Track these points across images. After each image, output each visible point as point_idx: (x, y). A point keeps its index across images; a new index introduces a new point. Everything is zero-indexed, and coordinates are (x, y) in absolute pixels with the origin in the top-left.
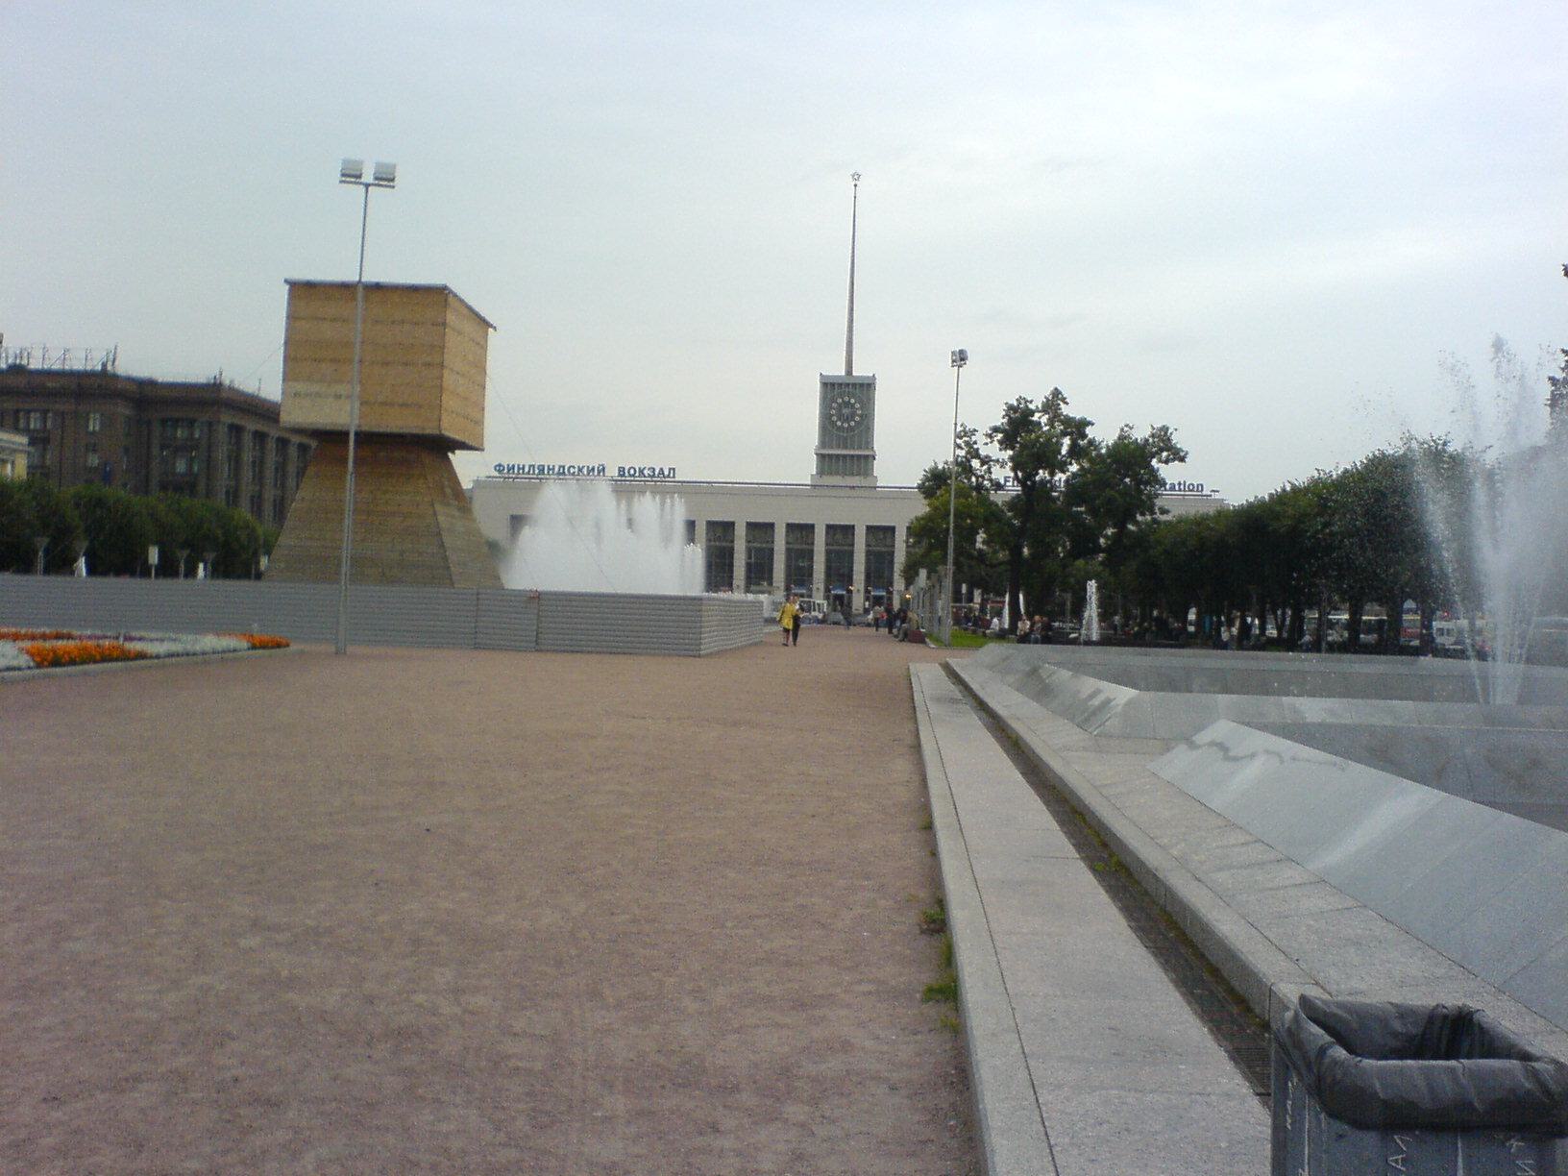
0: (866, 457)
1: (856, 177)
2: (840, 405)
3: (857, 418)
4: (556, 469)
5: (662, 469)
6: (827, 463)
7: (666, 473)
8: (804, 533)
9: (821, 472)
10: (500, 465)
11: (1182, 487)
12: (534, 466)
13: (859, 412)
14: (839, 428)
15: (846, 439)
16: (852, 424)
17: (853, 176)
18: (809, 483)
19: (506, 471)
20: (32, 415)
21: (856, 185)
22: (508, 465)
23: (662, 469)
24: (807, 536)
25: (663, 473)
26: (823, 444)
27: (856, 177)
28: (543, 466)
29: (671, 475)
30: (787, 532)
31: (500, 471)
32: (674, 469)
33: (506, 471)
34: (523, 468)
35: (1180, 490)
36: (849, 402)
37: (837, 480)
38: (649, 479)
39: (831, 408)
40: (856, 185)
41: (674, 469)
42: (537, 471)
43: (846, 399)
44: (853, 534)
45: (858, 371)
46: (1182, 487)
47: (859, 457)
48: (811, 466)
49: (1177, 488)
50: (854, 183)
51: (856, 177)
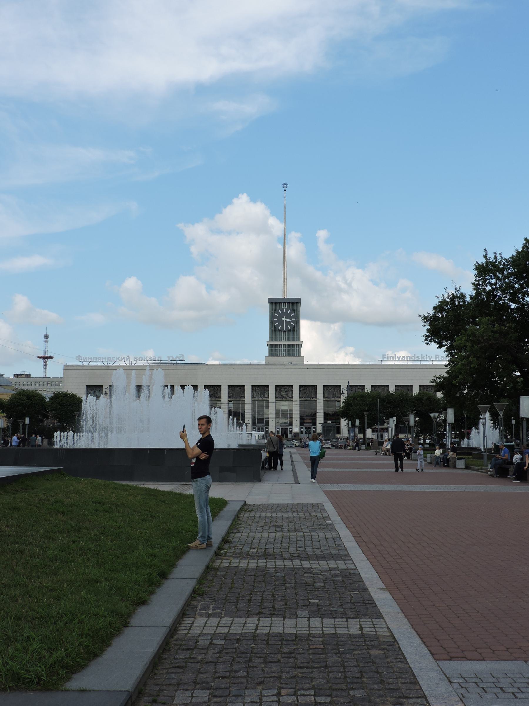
0: (297, 345)
9: (271, 354)
21: (285, 190)
24: (265, 393)
26: (271, 339)
40: (285, 190)
44: (292, 391)
45: (290, 295)
48: (266, 350)
50: (284, 189)
51: (285, 185)
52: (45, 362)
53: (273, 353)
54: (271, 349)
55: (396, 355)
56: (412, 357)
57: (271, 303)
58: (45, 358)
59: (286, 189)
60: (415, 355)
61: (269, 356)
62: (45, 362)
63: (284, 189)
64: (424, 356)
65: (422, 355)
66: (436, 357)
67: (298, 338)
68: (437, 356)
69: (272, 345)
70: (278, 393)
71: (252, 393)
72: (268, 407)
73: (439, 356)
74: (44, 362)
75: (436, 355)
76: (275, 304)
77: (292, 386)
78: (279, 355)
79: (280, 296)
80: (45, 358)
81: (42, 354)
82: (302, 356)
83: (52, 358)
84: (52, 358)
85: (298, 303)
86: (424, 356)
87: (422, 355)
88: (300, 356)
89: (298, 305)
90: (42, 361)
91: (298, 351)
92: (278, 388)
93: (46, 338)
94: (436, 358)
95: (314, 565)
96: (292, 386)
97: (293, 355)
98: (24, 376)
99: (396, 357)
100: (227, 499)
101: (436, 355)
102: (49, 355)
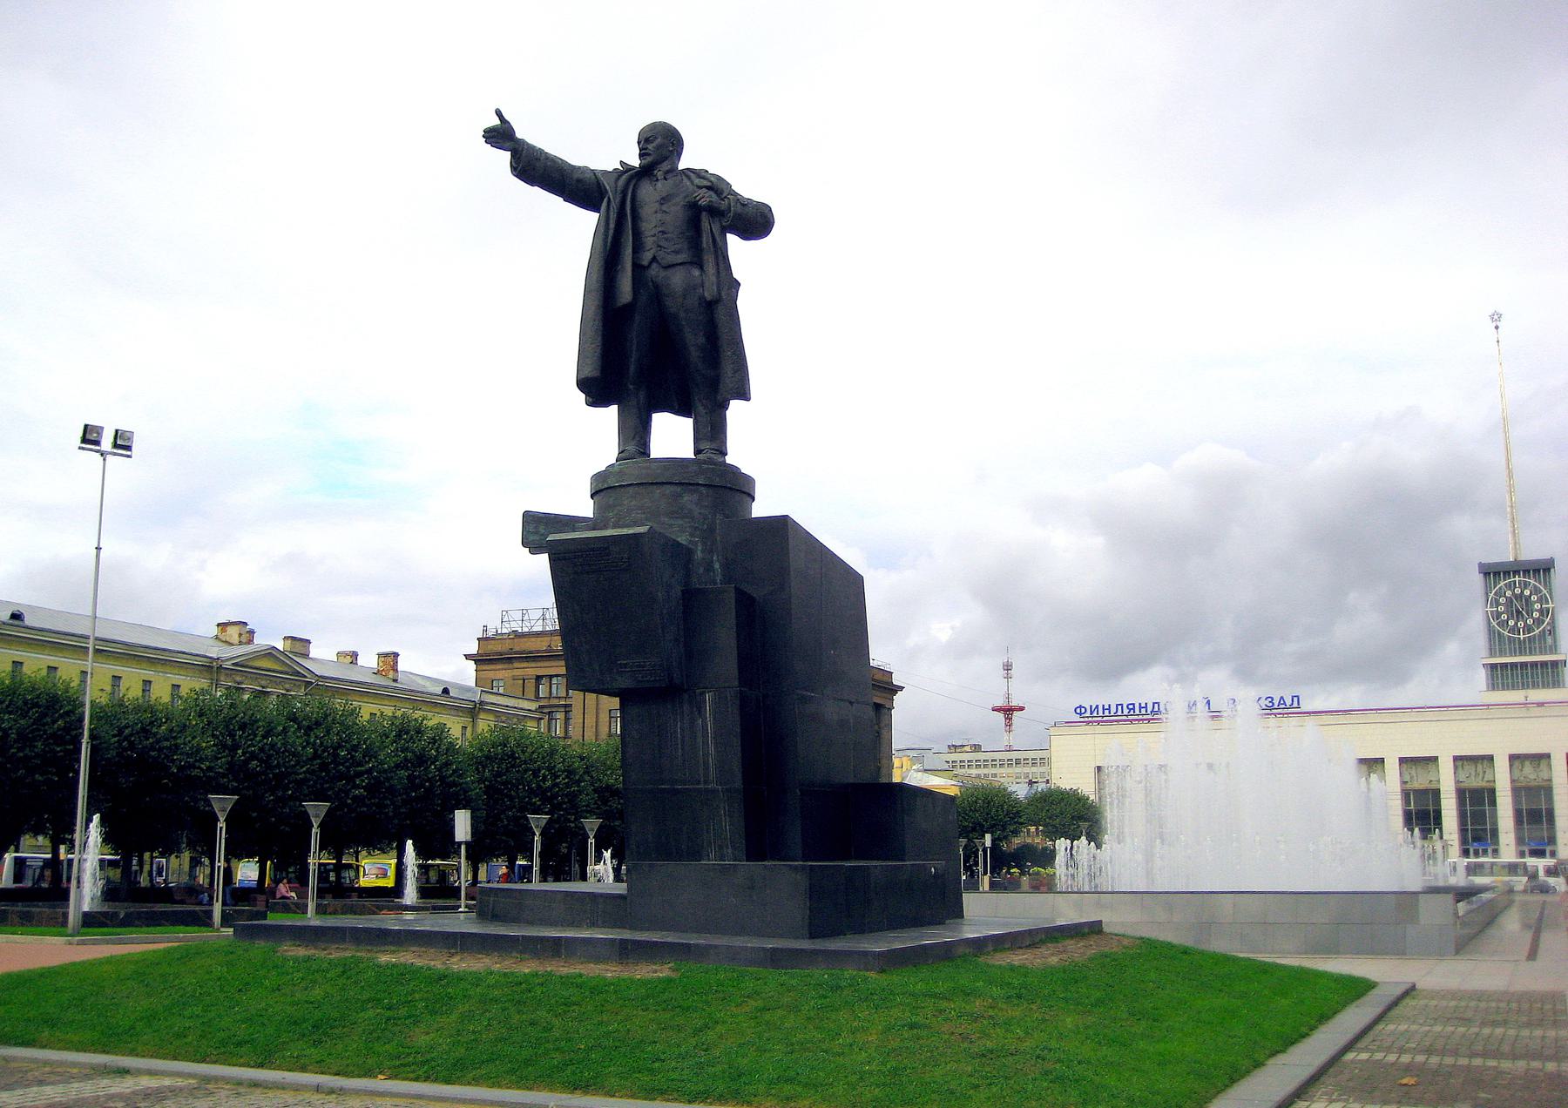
0: (1555, 664)
2: (1510, 601)
3: (1536, 615)
4: (1150, 709)
5: (1282, 698)
6: (1500, 676)
7: (1288, 702)
8: (1479, 766)
9: (1493, 686)
10: (1080, 707)
12: (1121, 705)
14: (1516, 629)
19: (1088, 714)
20: (554, 680)
22: (1091, 706)
23: (1282, 698)
25: (1285, 704)
27: (1496, 317)
28: (1133, 704)
29: (1295, 705)
30: (1456, 768)
31: (1081, 714)
32: (1298, 697)
33: (1088, 714)
34: (1109, 709)
36: (1522, 592)
38: (1269, 712)
39: (1498, 604)
41: (1298, 697)
42: (1126, 711)
43: (1517, 591)
45: (1532, 552)
47: (1544, 664)
48: (1481, 676)
52: (1009, 719)
53: (1508, 683)
57: (1487, 574)
58: (1008, 711)
62: (1009, 719)
67: (1554, 649)
69: (1493, 667)
70: (1517, 774)
71: (1455, 773)
72: (1493, 803)
74: (1006, 719)
76: (1494, 575)
80: (1008, 711)
81: (1000, 703)
83: (1022, 709)
84: (1022, 709)
85: (1549, 569)
89: (1550, 577)
90: (1001, 716)
91: (1558, 676)
92: (1517, 763)
93: (1007, 670)
95: (1506, 1065)
97: (1545, 685)
98: (968, 749)
100: (1377, 980)
102: (1014, 703)
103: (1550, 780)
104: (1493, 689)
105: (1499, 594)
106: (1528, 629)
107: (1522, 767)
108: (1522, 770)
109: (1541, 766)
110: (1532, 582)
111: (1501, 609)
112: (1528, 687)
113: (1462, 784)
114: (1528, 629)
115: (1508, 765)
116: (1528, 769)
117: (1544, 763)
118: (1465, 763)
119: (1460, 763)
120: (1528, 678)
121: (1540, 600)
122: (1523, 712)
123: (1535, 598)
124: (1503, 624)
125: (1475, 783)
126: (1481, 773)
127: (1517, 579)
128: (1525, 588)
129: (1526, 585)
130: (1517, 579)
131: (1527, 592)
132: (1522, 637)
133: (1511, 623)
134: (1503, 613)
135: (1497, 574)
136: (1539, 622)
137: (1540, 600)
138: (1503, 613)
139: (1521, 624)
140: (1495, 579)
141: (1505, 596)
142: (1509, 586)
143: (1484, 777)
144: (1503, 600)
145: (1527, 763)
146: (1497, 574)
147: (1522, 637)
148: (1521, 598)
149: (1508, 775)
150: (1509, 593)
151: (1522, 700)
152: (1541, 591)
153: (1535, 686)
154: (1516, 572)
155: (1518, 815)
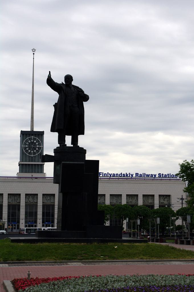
1: (34, 50)
3: (37, 149)
6: (23, 167)
8: (16, 197)
11: (169, 176)
13: (38, 146)
14: (30, 153)
15: (32, 157)
16: (35, 151)
17: (32, 50)
18: (16, 176)
21: (34, 54)
26: (22, 159)
30: (8, 197)
35: (168, 177)
36: (34, 141)
37: (29, 175)
39: (26, 145)
40: (34, 54)
43: (32, 141)
44: (37, 198)
45: (36, 129)
46: (169, 176)
48: (17, 169)
49: (167, 176)
50: (33, 53)
54: (22, 168)
55: (109, 173)
56: (120, 174)
59: (34, 53)
60: (121, 173)
61: (19, 172)
63: (33, 53)
64: (128, 174)
65: (126, 173)
66: (136, 175)
68: (137, 174)
70: (27, 200)
72: (19, 210)
73: (138, 174)
75: (136, 174)
77: (37, 195)
78: (28, 172)
79: (29, 129)
82: (44, 173)
85: (42, 135)
86: (128, 174)
87: (126, 173)
88: (43, 173)
91: (42, 169)
92: (27, 197)
94: (136, 176)
96: (37, 195)
97: (38, 172)
99: (109, 174)
101: (136, 174)
103: (37, 203)
104: (22, 172)
105: (27, 141)
106: (34, 153)
107: (29, 198)
108: (29, 199)
109: (35, 198)
110: (37, 138)
111: (27, 146)
112: (32, 172)
113: (44, 203)
114: (34, 153)
115: (7, 197)
116: (31, 199)
117: (36, 196)
118: (11, 196)
119: (10, 196)
120: (33, 169)
121: (39, 145)
122: (31, 180)
123: (37, 143)
124: (27, 151)
125: (14, 203)
126: (16, 200)
127: (32, 137)
128: (35, 140)
129: (35, 139)
130: (32, 137)
131: (35, 142)
132: (32, 156)
133: (29, 151)
134: (27, 147)
135: (26, 135)
136: (38, 151)
137: (39, 145)
138: (27, 147)
139: (32, 152)
140: (26, 136)
141: (28, 142)
142: (30, 139)
143: (17, 201)
144: (28, 143)
145: (31, 197)
146: (27, 134)
147: (32, 156)
148: (33, 143)
149: (25, 200)
150: (29, 141)
151: (31, 176)
152: (39, 141)
153: (35, 172)
154: (32, 135)
155: (26, 213)
